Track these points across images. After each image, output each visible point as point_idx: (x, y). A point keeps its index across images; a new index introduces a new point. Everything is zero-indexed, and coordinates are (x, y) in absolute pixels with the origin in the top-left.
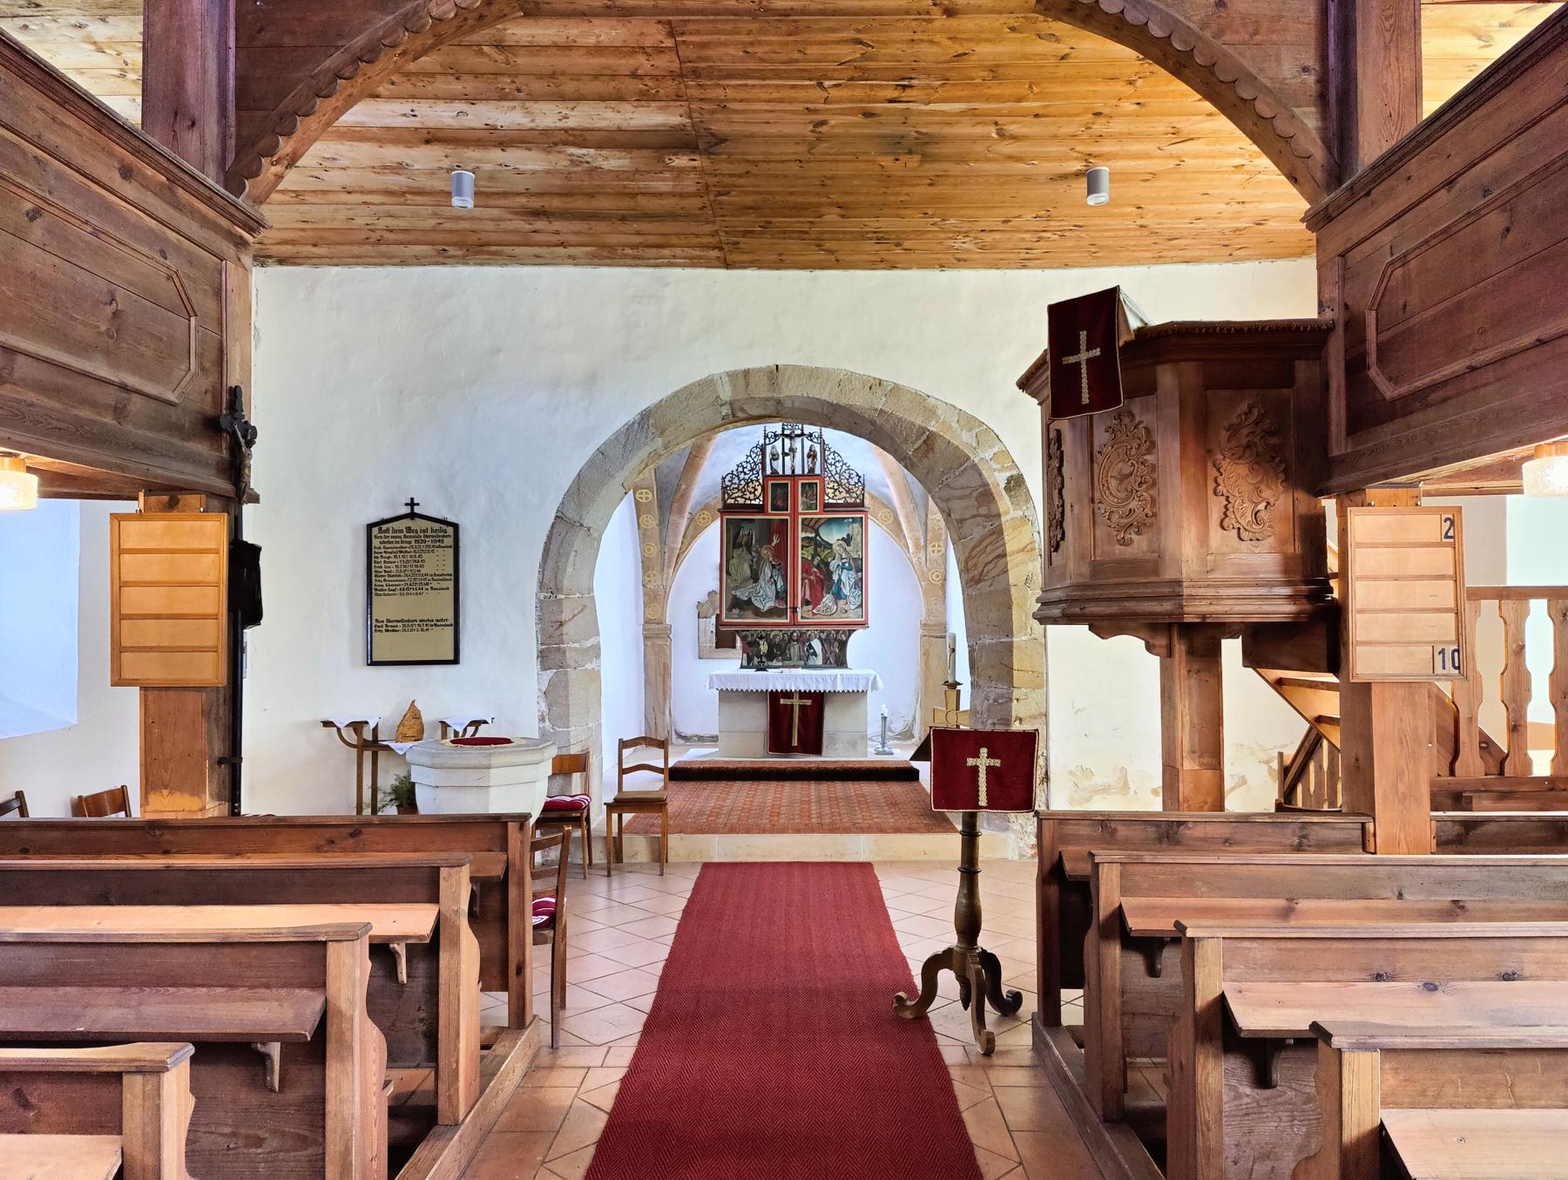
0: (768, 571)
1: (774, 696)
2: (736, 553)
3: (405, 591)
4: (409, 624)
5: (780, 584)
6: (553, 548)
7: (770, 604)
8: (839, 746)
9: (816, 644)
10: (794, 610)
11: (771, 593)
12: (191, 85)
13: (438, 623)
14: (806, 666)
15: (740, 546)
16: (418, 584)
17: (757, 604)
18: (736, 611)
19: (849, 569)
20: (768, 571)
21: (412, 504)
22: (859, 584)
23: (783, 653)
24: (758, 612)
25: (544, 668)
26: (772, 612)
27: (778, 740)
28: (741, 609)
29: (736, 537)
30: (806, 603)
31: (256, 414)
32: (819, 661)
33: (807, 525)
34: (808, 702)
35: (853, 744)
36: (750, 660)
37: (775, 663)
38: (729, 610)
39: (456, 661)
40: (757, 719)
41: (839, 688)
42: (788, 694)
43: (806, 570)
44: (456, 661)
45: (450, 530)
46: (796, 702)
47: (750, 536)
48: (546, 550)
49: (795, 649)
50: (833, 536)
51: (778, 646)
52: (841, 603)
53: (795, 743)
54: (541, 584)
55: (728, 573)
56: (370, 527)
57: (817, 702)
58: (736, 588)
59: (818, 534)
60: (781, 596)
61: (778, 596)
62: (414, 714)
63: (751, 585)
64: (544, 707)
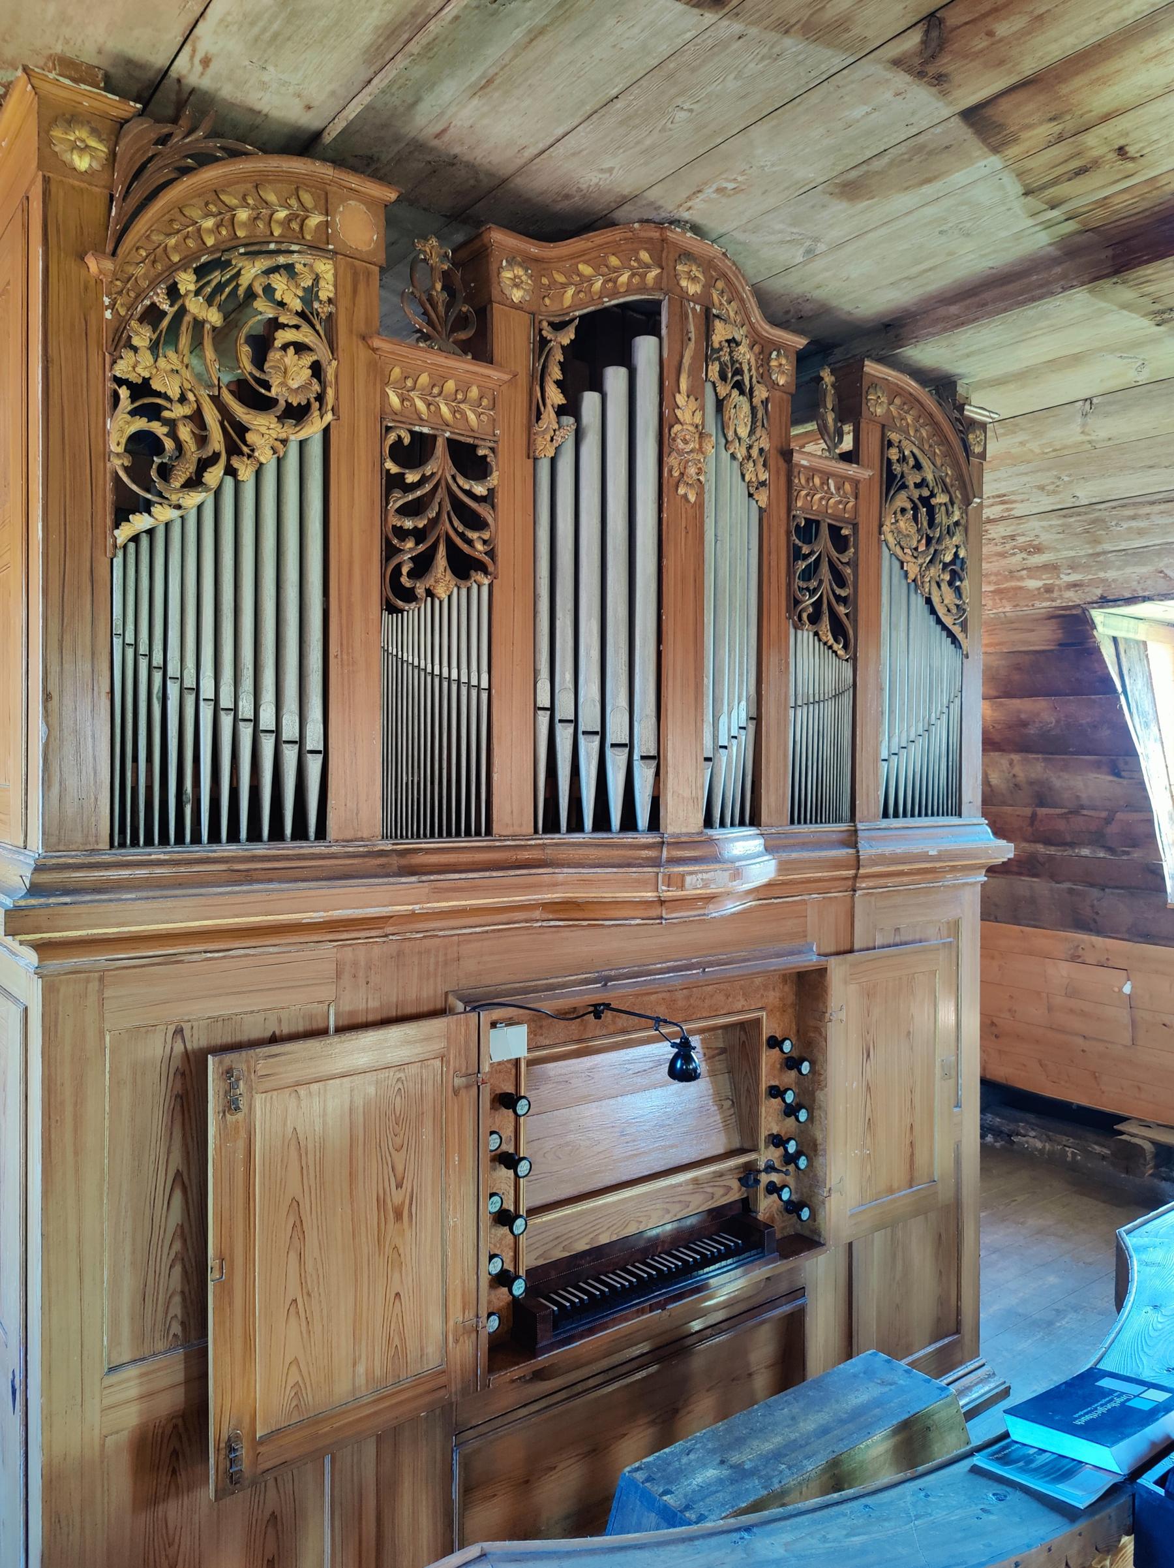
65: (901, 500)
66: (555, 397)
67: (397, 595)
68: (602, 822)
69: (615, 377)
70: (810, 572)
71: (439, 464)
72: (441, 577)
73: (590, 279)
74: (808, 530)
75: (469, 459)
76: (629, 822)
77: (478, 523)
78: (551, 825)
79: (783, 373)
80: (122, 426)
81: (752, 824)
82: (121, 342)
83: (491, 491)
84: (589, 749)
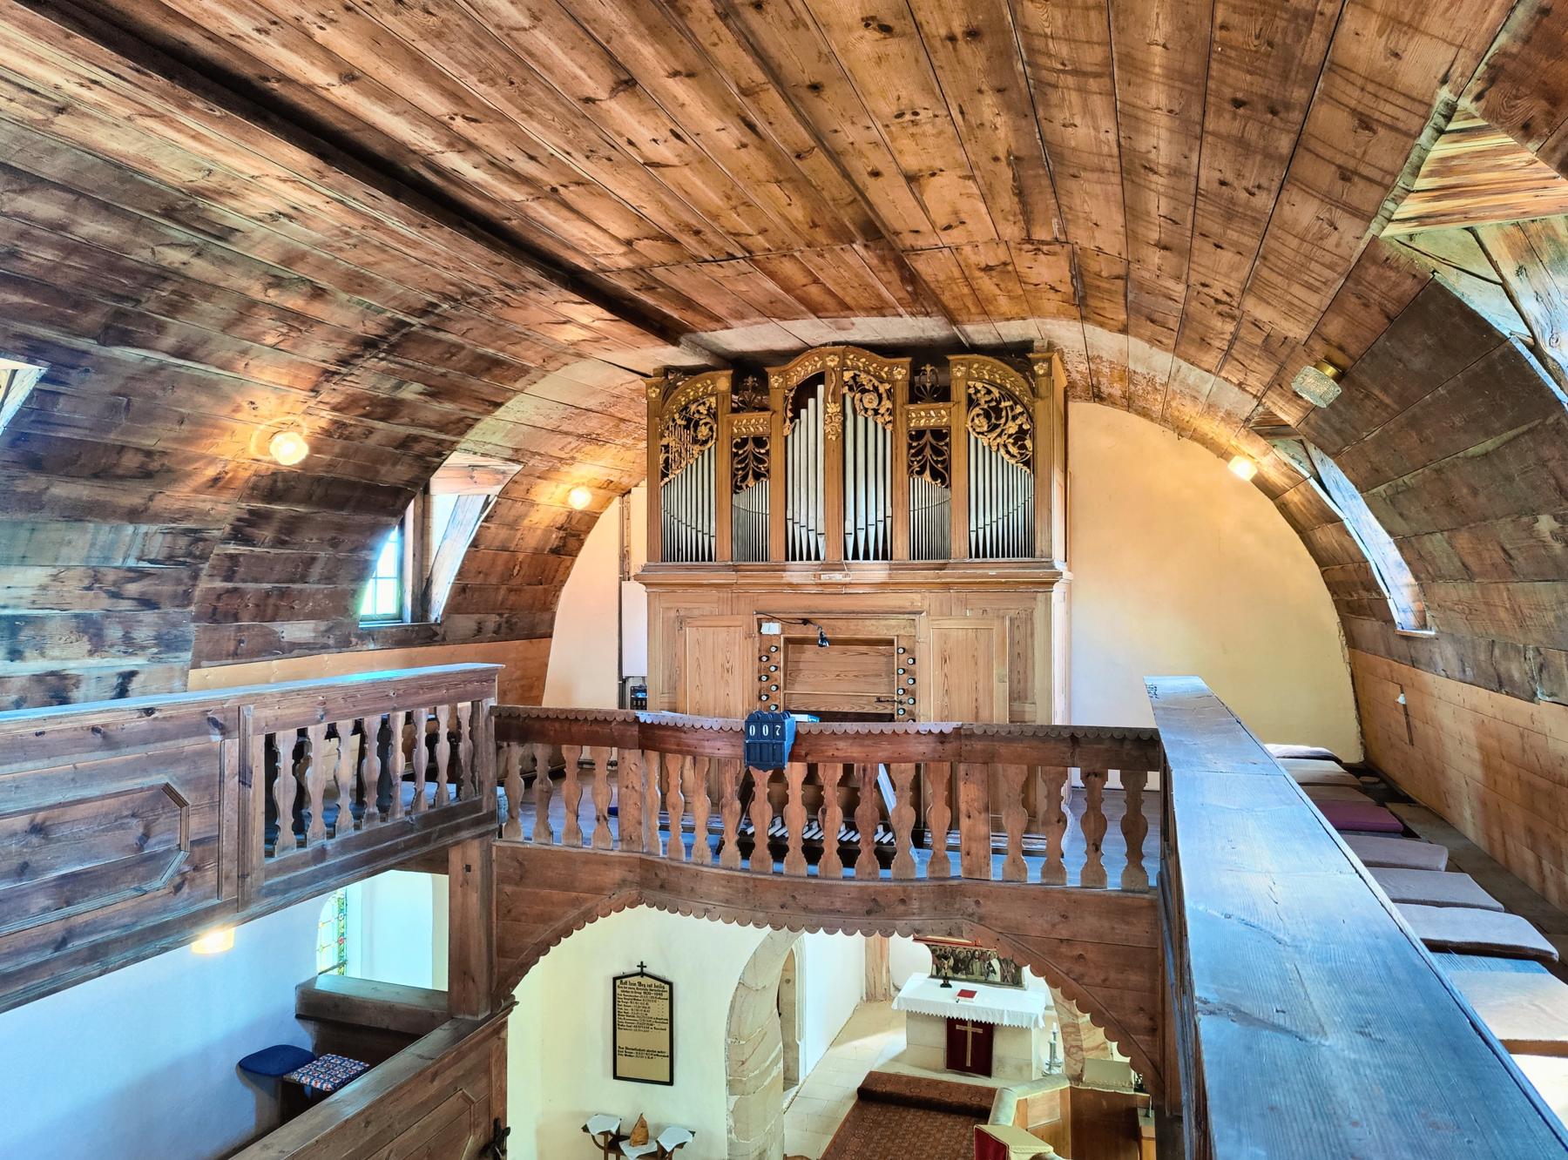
1: (952, 1023)
3: (639, 1027)
4: (640, 1052)
6: (737, 1005)
8: (1008, 1069)
9: (995, 963)
12: (473, 961)
13: (659, 1054)
14: (986, 982)
16: (646, 1024)
21: (642, 966)
23: (967, 968)
25: (732, 1093)
27: (955, 1061)
31: (510, 1122)
32: (998, 978)
34: (980, 1031)
35: (1020, 1069)
36: (938, 970)
37: (959, 976)
39: (671, 1083)
40: (939, 1037)
41: (1006, 1022)
42: (963, 1022)
44: (671, 1083)
45: (667, 987)
46: (969, 1029)
48: (732, 1007)
49: (977, 966)
51: (963, 961)
53: (969, 1064)
54: (729, 1032)
56: (615, 979)
57: (986, 1032)
62: (642, 1124)
64: (731, 1122)
65: (977, 410)
66: (790, 415)
67: (736, 489)
68: (809, 558)
69: (811, 401)
70: (920, 452)
71: (750, 446)
72: (751, 481)
73: (801, 371)
74: (920, 434)
75: (759, 442)
76: (817, 558)
77: (762, 461)
78: (794, 559)
79: (900, 373)
80: (662, 457)
81: (885, 557)
82: (662, 436)
83: (767, 453)
84: (804, 530)
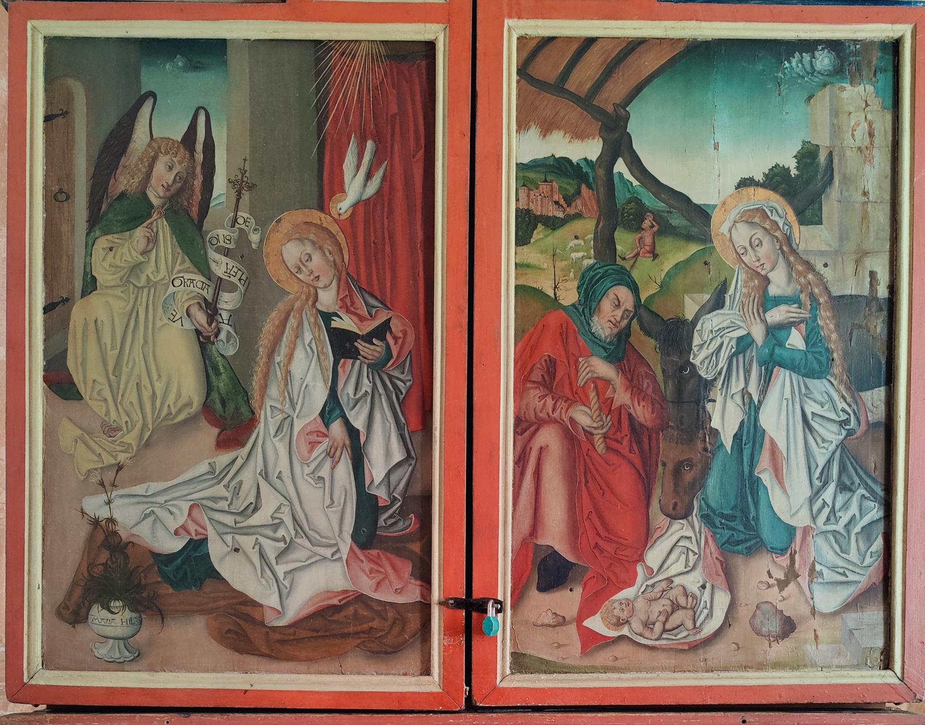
0: (305, 372)
2: (111, 257)
5: (384, 453)
7: (320, 577)
10: (471, 608)
11: (328, 507)
15: (136, 212)
17: (239, 574)
18: (111, 621)
19: (811, 367)
20: (305, 372)
22: (873, 458)
24: (244, 630)
26: (331, 629)
28: (146, 604)
29: (114, 147)
30: (550, 572)
33: (553, 79)
38: (71, 611)
43: (546, 372)
47: (196, 146)
50: (708, 155)
52: (758, 572)
55: (60, 384)
58: (111, 479)
59: (619, 143)
60: (387, 527)
61: (367, 533)
63: (200, 451)
